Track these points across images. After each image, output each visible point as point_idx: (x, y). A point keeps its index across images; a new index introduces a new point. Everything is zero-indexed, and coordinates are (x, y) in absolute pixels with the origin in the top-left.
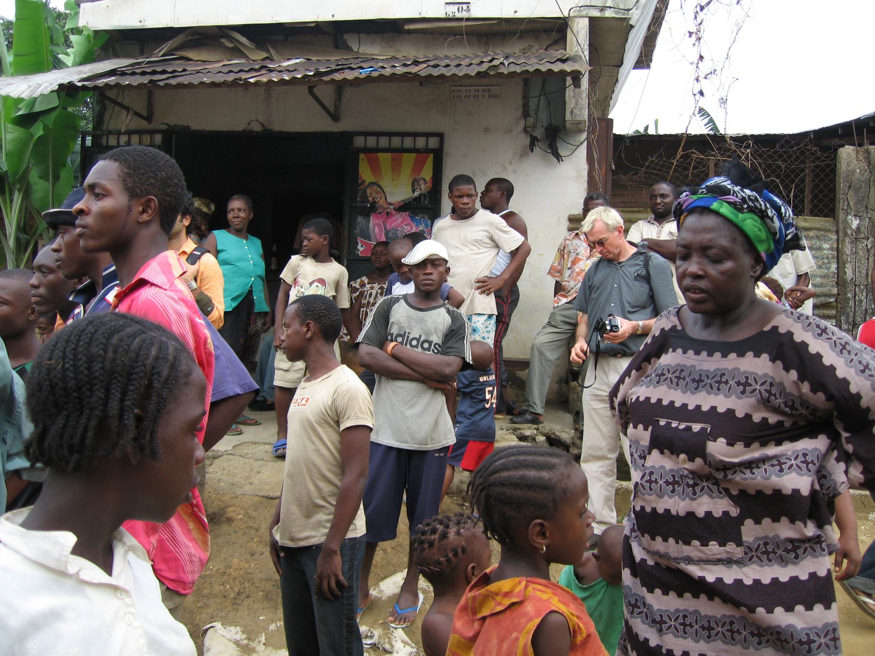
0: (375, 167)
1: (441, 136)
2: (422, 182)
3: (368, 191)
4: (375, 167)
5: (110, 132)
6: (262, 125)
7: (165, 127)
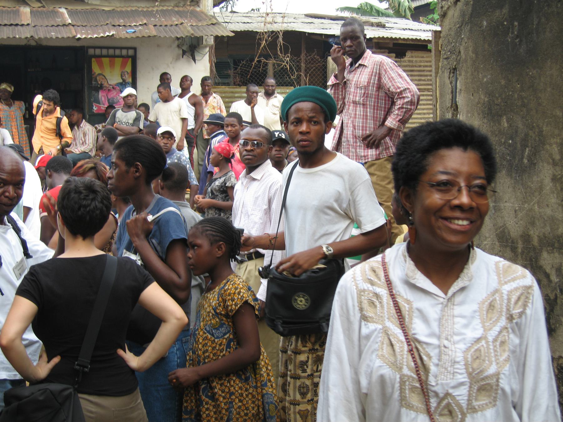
0: (101, 65)
1: (135, 49)
2: (126, 73)
3: (98, 78)
4: (101, 65)
6: (36, 42)
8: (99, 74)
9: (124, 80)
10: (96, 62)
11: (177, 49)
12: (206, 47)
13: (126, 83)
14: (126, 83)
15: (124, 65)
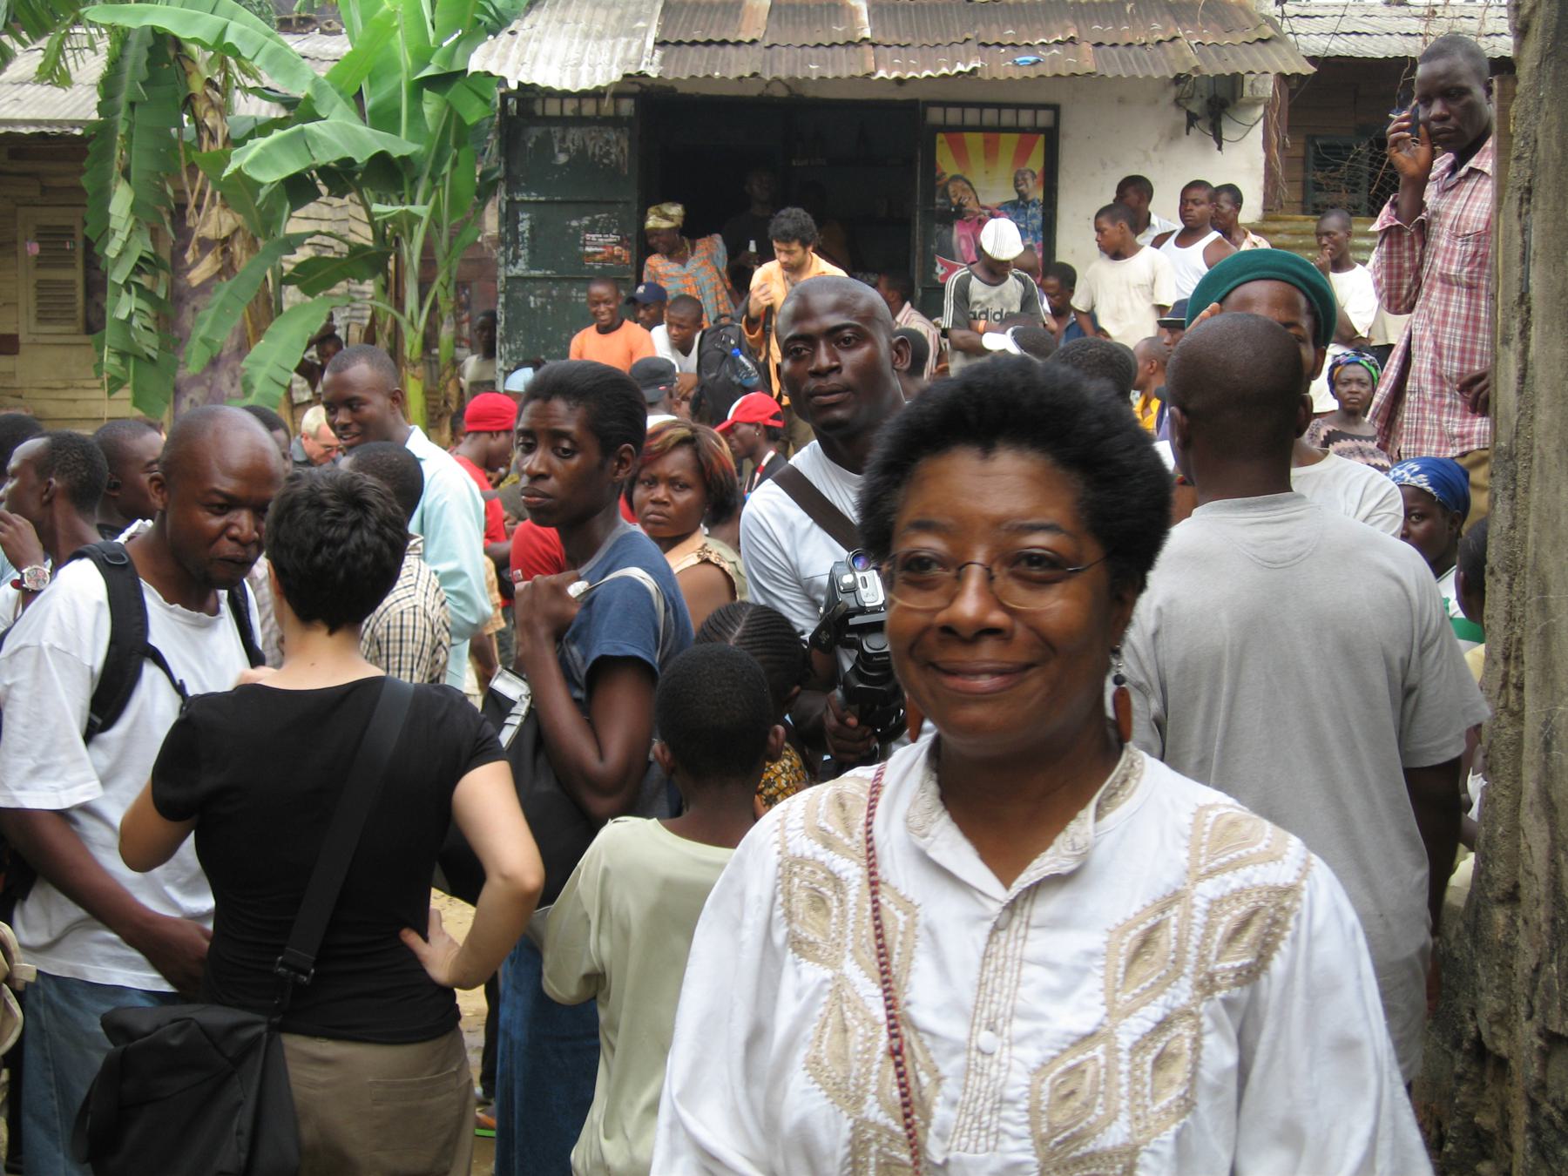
0: (960, 153)
1: (1055, 109)
2: (1028, 176)
3: (951, 188)
4: (960, 153)
8: (955, 178)
9: (1022, 196)
10: (946, 145)
11: (1173, 109)
12: (1254, 103)
13: (1028, 203)
14: (1028, 203)
15: (1023, 153)
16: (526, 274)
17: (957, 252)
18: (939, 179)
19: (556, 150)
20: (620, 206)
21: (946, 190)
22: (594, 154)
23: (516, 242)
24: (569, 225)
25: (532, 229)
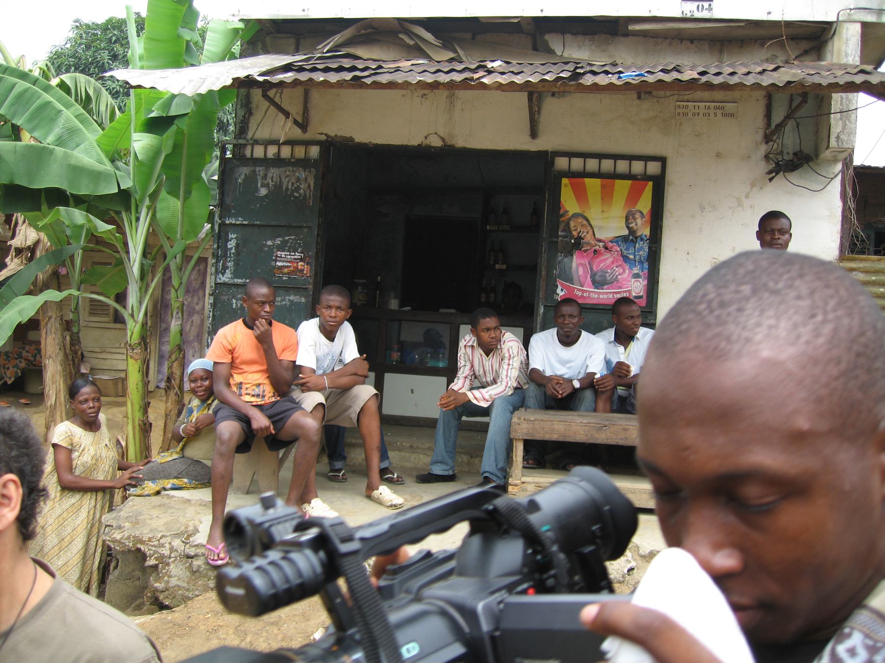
0: (581, 195)
1: (663, 160)
2: (638, 216)
3: (572, 224)
4: (581, 195)
5: (256, 142)
6: (443, 139)
7: (324, 138)
8: (576, 215)
9: (632, 232)
10: (570, 187)
13: (636, 238)
14: (636, 238)
16: (231, 282)
17: (575, 277)
18: (562, 216)
19: (259, 185)
20: (305, 230)
21: (568, 224)
22: (287, 188)
23: (225, 256)
24: (266, 245)
25: (237, 246)
